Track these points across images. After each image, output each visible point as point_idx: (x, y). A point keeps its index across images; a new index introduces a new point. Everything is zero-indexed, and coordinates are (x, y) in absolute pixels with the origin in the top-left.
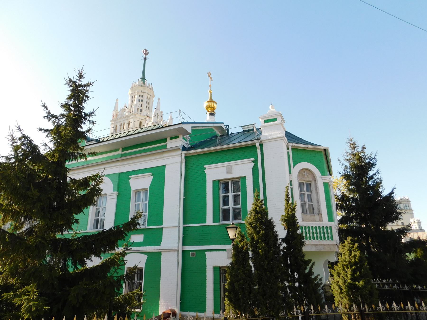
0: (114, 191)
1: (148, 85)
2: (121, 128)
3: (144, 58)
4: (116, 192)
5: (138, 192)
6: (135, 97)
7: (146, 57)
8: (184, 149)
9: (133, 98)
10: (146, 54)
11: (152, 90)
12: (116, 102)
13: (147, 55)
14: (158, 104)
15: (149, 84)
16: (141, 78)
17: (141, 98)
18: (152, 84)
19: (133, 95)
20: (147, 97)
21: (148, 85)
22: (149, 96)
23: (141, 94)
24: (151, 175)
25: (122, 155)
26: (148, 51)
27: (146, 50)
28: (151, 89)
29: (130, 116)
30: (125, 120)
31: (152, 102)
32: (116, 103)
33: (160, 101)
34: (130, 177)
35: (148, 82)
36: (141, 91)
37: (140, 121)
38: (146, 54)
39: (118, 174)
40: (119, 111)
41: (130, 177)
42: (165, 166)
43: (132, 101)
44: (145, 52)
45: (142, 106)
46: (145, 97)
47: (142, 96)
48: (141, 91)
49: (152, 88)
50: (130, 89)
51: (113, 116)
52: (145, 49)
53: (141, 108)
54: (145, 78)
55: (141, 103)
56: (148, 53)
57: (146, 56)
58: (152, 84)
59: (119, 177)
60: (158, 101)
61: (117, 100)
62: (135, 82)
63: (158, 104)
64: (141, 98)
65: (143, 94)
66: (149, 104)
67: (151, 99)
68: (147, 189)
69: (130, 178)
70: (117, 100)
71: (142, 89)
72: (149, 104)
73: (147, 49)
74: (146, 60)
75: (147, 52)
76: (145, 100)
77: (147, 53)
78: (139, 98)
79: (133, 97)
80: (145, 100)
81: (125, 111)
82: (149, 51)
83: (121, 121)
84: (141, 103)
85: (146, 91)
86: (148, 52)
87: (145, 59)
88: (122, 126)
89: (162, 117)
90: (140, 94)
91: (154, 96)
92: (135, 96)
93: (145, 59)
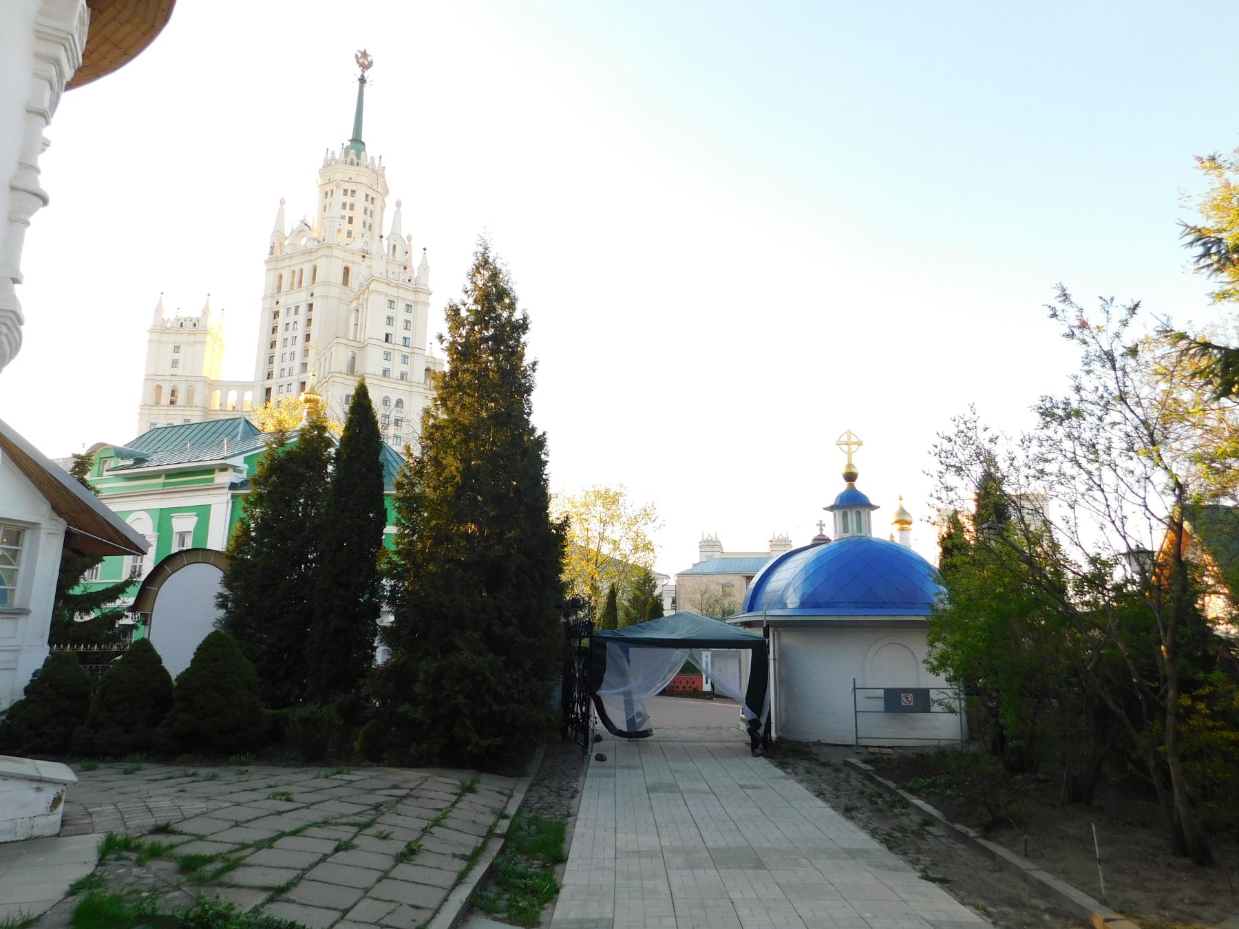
0: (153, 532)
1: (369, 161)
2: (292, 284)
3: (359, 79)
4: (155, 533)
5: (182, 536)
6: (332, 195)
7: (365, 75)
8: (233, 486)
9: (326, 197)
10: (365, 66)
11: (382, 175)
12: (279, 207)
13: (369, 68)
14: (397, 216)
15: (373, 159)
16: (351, 138)
17: (349, 200)
18: (380, 157)
19: (329, 188)
20: (367, 196)
21: (369, 161)
22: (372, 194)
23: (350, 187)
24: (196, 515)
25: (165, 485)
26: (370, 56)
27: (365, 54)
28: (379, 173)
29: (317, 250)
30: (303, 262)
31: (382, 209)
32: (280, 210)
33: (402, 209)
34: (172, 515)
35: (371, 150)
36: (350, 178)
37: (346, 264)
38: (365, 66)
39: (158, 511)
40: (287, 234)
41: (172, 515)
42: (210, 505)
43: (325, 207)
44: (361, 60)
45: (351, 220)
46: (360, 195)
47: (353, 192)
48: (350, 178)
49: (381, 172)
50: (320, 170)
51: (272, 247)
52: (363, 51)
53: (350, 227)
54: (363, 140)
55: (348, 213)
56: (371, 64)
57: (366, 74)
58: (380, 157)
59: (160, 513)
60: (395, 208)
61: (282, 202)
62: (333, 153)
63: (397, 216)
64: (349, 200)
65: (354, 189)
66: (371, 216)
67: (378, 202)
68: (191, 532)
69: (173, 517)
70: (282, 202)
71: (351, 171)
72: (371, 216)
73: (367, 52)
74: (365, 85)
75: (367, 60)
76: (360, 202)
77: (367, 63)
78: (345, 199)
79: (327, 193)
80: (360, 202)
81: (304, 236)
82: (374, 56)
83: (292, 263)
84: (348, 213)
85: (363, 180)
86: (372, 61)
87: (362, 81)
88: (296, 279)
89: (407, 253)
90: (346, 188)
91: (386, 191)
92: (332, 192)
93: (362, 81)
